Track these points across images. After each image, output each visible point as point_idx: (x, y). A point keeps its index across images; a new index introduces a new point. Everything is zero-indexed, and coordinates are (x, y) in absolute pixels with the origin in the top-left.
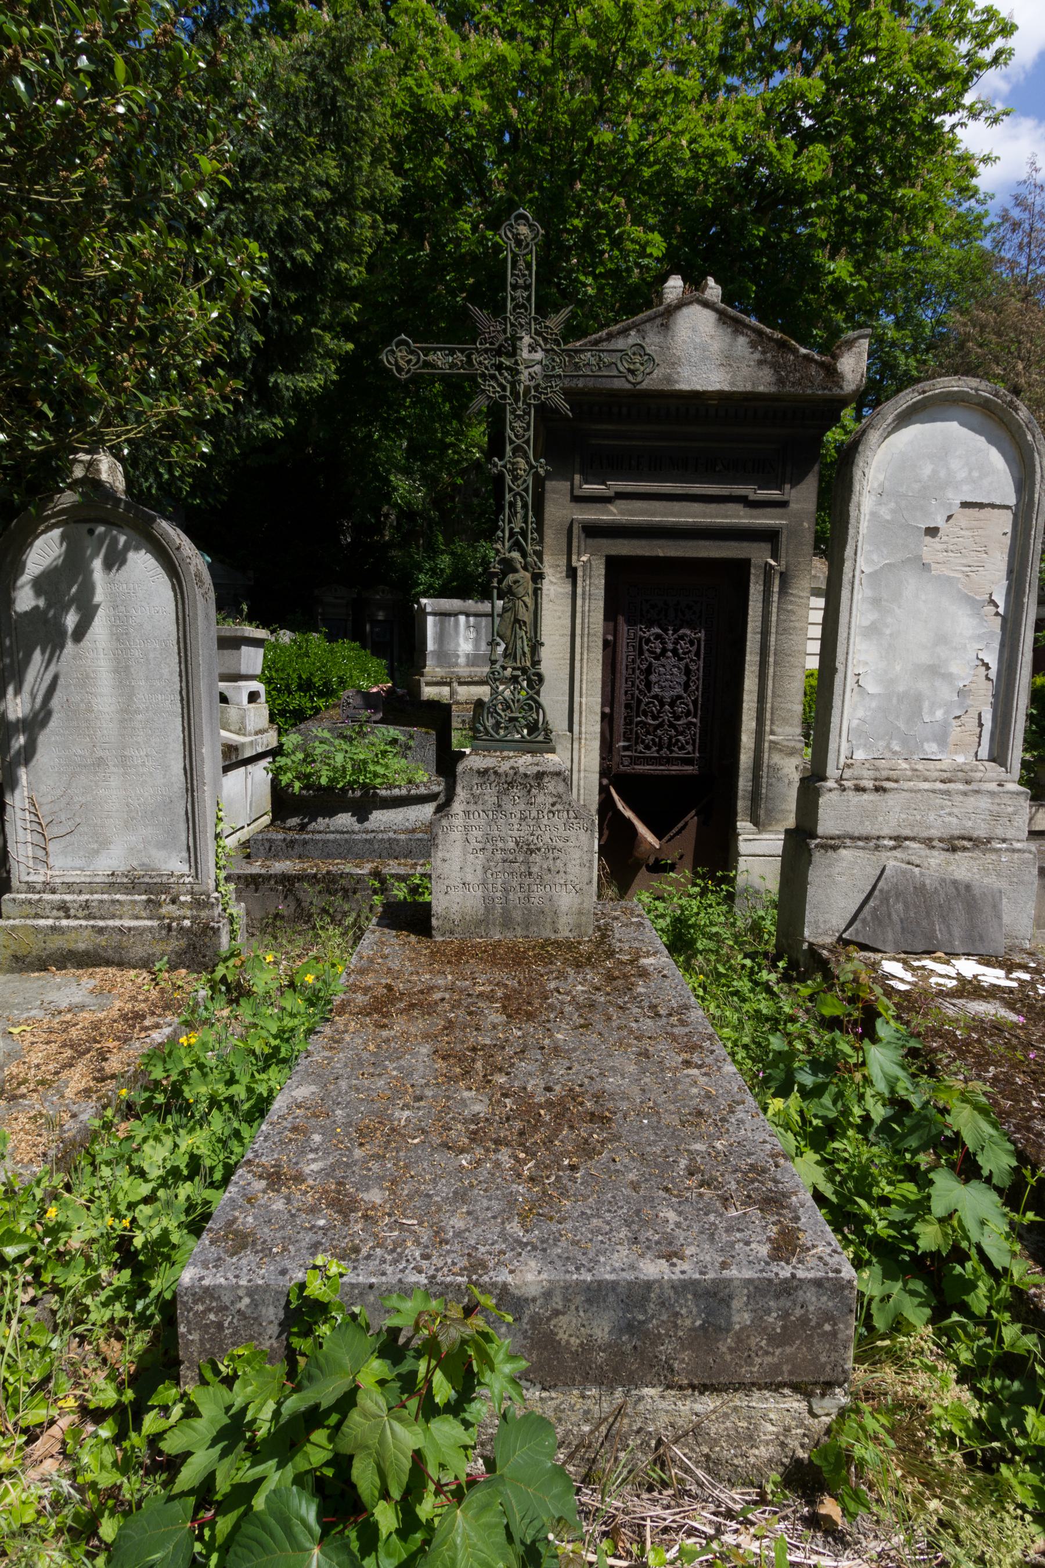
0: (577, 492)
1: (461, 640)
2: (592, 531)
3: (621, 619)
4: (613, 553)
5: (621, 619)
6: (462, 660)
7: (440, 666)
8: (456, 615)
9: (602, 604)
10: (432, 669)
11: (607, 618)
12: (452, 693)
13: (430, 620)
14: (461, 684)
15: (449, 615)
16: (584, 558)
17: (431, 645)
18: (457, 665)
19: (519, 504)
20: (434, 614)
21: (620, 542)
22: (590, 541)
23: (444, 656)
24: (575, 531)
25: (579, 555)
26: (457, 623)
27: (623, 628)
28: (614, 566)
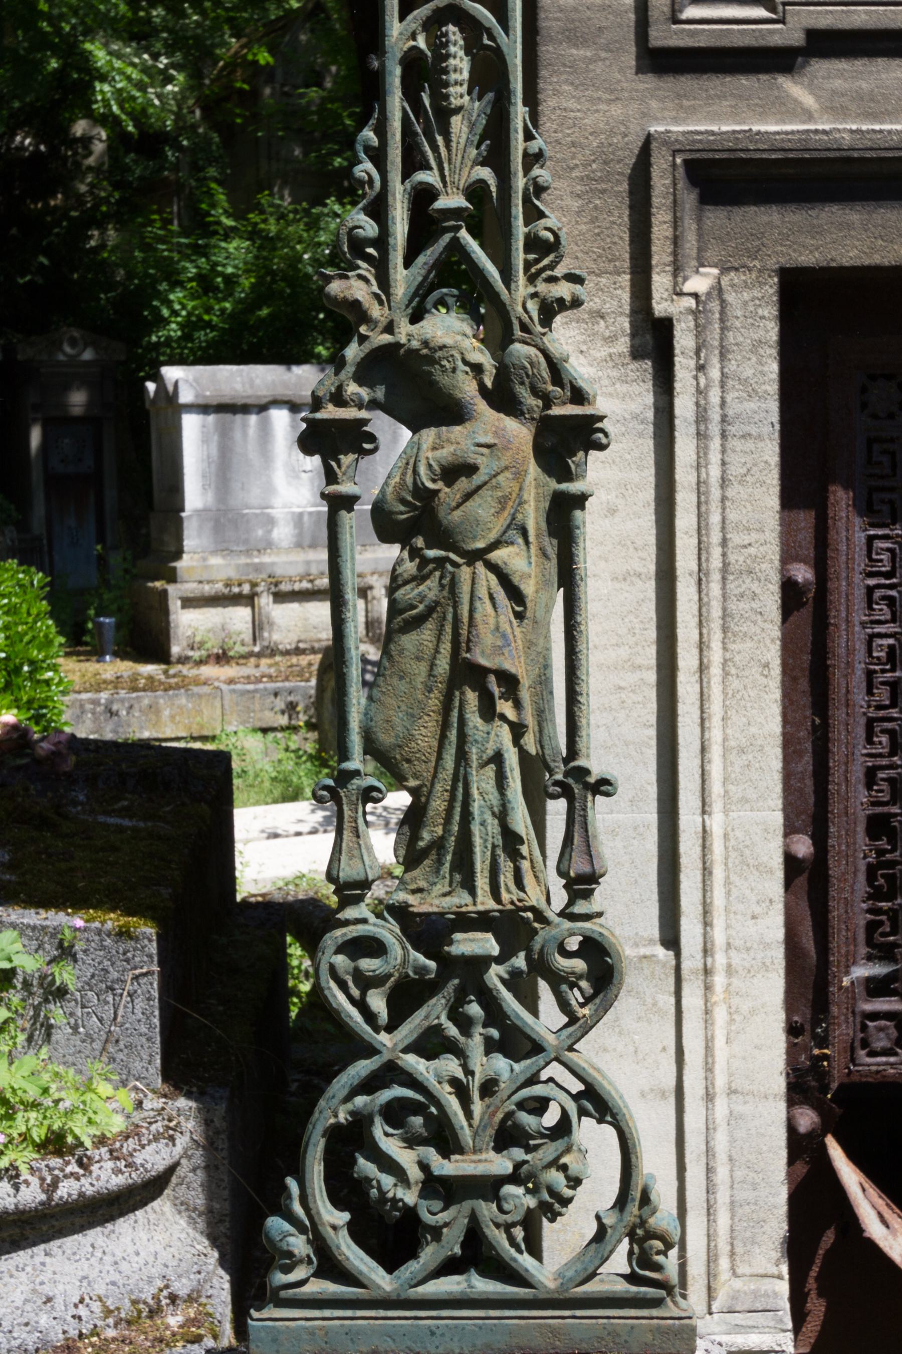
0: (663, 36)
1: (279, 477)
2: (727, 179)
3: (841, 499)
4: (807, 259)
5: (841, 499)
6: (283, 533)
7: (223, 549)
8: (262, 408)
9: (770, 452)
10: (200, 560)
11: (791, 497)
12: (258, 626)
13: (192, 427)
14: (280, 597)
15: (244, 409)
16: (699, 283)
17: (195, 494)
18: (268, 545)
19: (460, 65)
20: (204, 409)
21: (830, 214)
22: (716, 217)
23: (228, 523)
24: (661, 182)
25: (677, 270)
26: (265, 431)
27: (851, 531)
28: (811, 305)
